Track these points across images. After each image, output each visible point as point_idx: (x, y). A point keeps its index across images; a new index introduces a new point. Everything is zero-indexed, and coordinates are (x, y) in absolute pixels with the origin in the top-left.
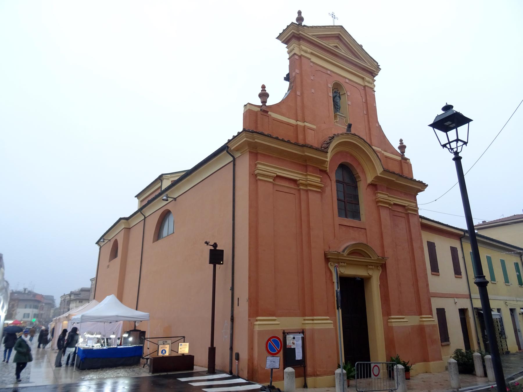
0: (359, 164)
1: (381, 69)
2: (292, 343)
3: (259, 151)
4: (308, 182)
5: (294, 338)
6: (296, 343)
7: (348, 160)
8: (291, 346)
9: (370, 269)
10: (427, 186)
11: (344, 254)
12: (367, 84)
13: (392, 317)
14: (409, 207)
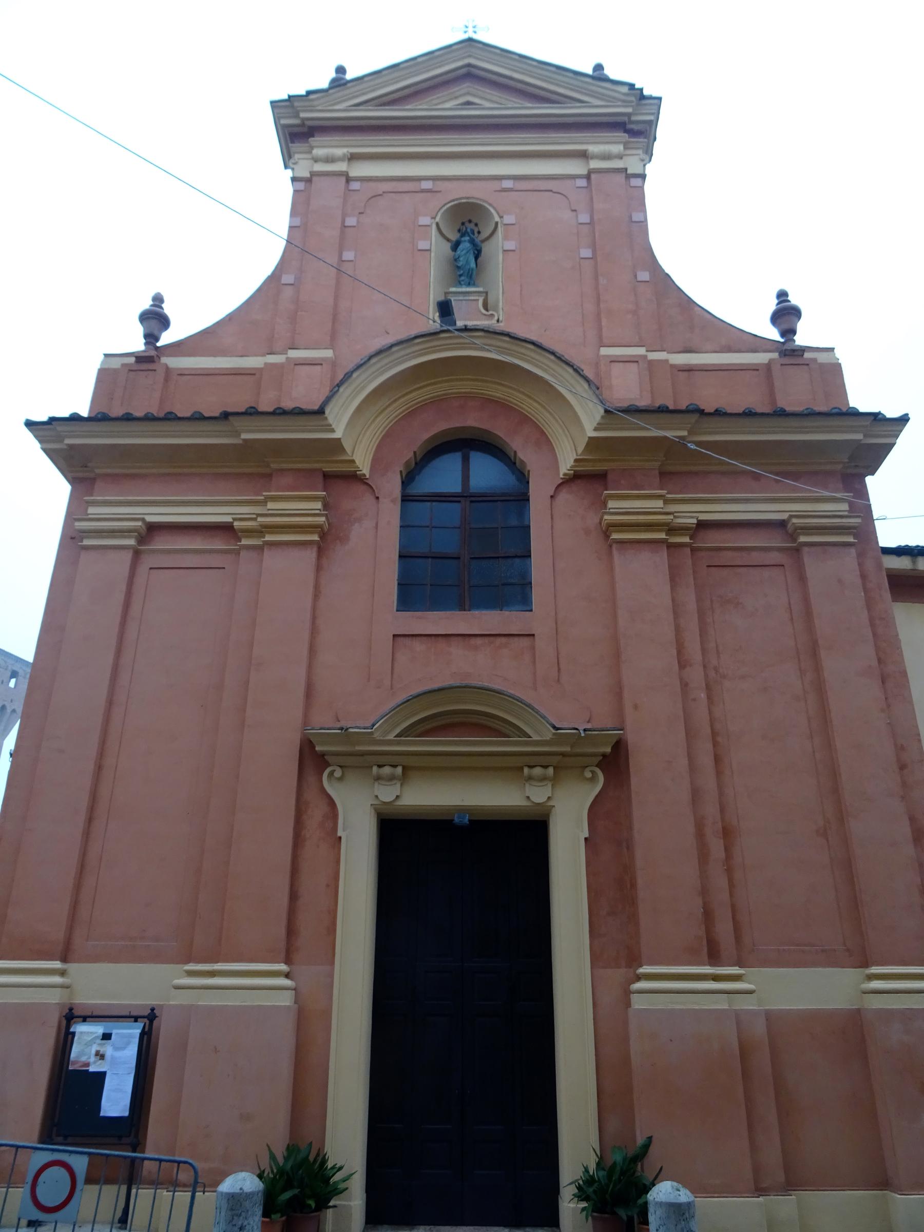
0: (525, 420)
1: (660, 99)
2: (93, 1052)
3: (97, 471)
4: (259, 519)
5: (107, 1037)
6: (113, 1057)
7: (473, 420)
8: (88, 1065)
9: (530, 778)
10: (904, 420)
11: (372, 733)
12: (594, 164)
13: (645, 969)
14: (795, 520)
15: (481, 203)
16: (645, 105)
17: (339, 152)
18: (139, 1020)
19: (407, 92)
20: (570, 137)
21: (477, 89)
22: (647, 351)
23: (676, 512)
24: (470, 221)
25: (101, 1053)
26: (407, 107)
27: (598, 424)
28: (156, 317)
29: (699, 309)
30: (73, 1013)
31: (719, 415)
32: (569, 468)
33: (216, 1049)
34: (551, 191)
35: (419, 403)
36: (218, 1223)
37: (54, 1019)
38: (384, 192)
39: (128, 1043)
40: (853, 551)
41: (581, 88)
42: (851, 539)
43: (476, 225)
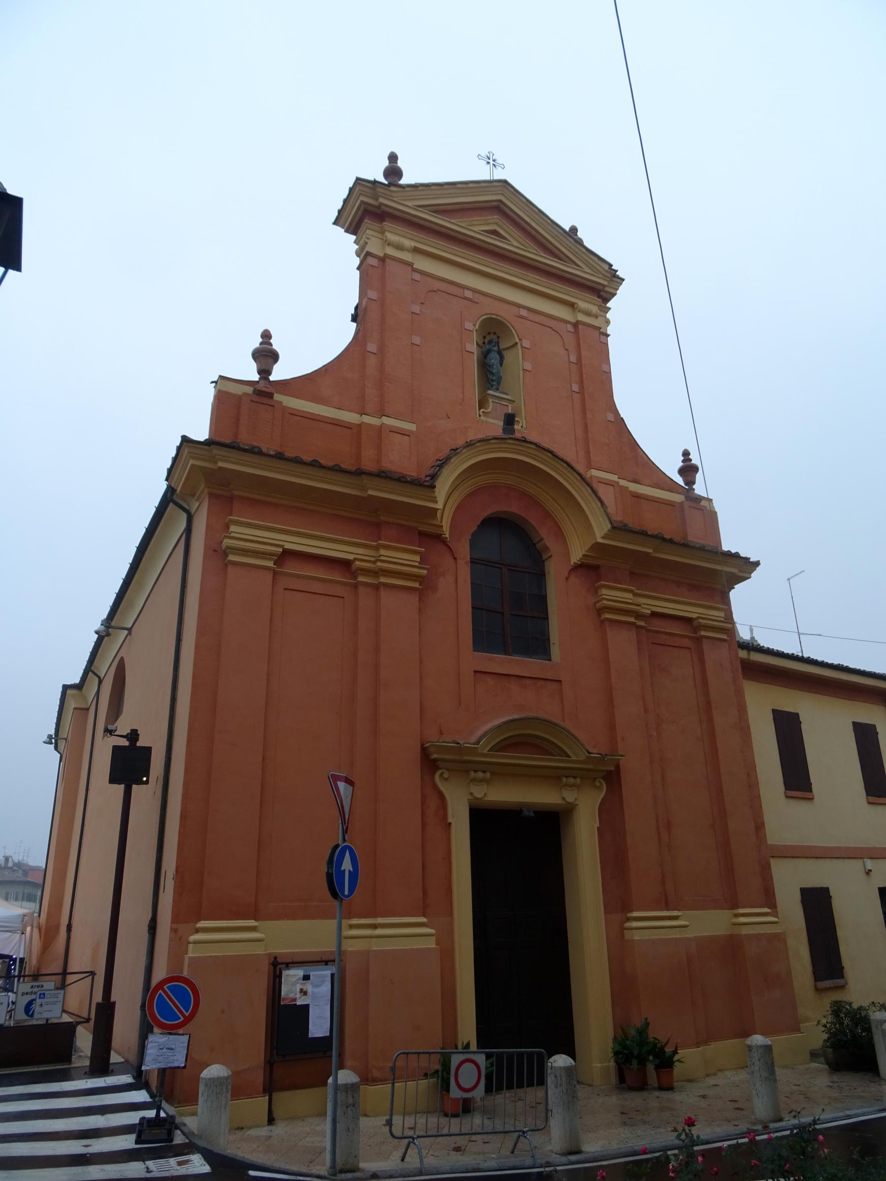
0: (548, 515)
1: (623, 280)
2: (298, 990)
3: (236, 493)
4: (379, 564)
5: (306, 978)
6: (313, 993)
7: (514, 507)
8: (295, 1000)
9: (566, 785)
10: (757, 564)
11: (477, 748)
12: (581, 317)
13: (635, 914)
14: (701, 621)
15: (507, 323)
16: (613, 281)
17: (408, 243)
18: (329, 963)
19: (457, 207)
20: (567, 290)
21: (504, 223)
22: (619, 478)
23: (643, 604)
24: (495, 333)
25: (304, 990)
26: (452, 221)
27: (605, 534)
28: (273, 356)
29: (641, 451)
30: (277, 961)
31: (671, 542)
32: (578, 559)
33: (392, 982)
34: (552, 328)
35: (479, 486)
36: (560, 1085)
37: (265, 967)
38: (438, 290)
39: (323, 982)
40: (726, 644)
41: (564, 242)
42: (724, 637)
43: (498, 337)
